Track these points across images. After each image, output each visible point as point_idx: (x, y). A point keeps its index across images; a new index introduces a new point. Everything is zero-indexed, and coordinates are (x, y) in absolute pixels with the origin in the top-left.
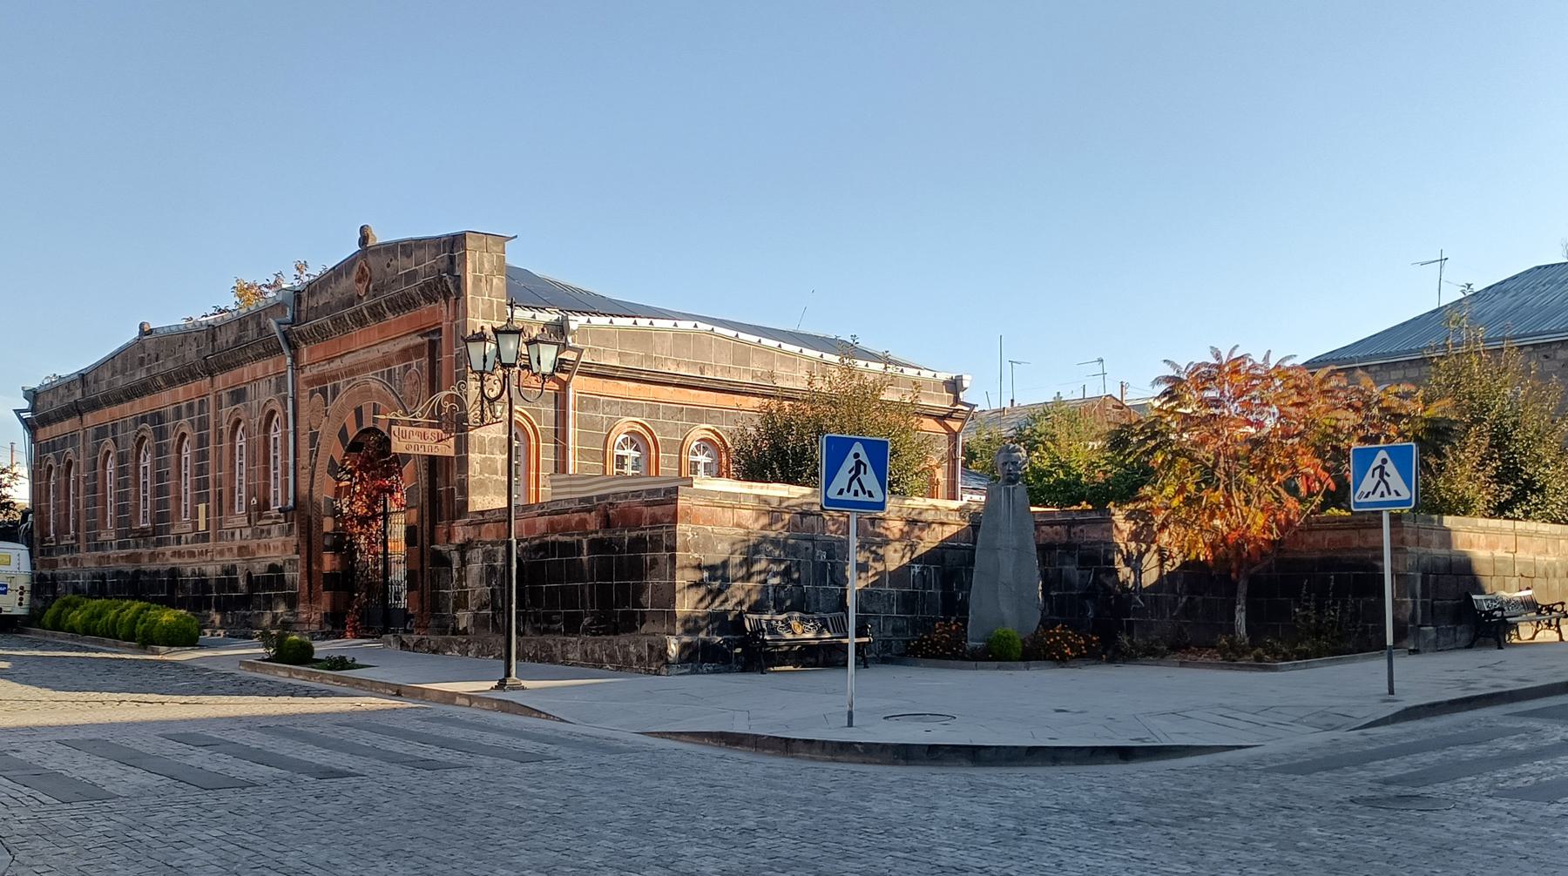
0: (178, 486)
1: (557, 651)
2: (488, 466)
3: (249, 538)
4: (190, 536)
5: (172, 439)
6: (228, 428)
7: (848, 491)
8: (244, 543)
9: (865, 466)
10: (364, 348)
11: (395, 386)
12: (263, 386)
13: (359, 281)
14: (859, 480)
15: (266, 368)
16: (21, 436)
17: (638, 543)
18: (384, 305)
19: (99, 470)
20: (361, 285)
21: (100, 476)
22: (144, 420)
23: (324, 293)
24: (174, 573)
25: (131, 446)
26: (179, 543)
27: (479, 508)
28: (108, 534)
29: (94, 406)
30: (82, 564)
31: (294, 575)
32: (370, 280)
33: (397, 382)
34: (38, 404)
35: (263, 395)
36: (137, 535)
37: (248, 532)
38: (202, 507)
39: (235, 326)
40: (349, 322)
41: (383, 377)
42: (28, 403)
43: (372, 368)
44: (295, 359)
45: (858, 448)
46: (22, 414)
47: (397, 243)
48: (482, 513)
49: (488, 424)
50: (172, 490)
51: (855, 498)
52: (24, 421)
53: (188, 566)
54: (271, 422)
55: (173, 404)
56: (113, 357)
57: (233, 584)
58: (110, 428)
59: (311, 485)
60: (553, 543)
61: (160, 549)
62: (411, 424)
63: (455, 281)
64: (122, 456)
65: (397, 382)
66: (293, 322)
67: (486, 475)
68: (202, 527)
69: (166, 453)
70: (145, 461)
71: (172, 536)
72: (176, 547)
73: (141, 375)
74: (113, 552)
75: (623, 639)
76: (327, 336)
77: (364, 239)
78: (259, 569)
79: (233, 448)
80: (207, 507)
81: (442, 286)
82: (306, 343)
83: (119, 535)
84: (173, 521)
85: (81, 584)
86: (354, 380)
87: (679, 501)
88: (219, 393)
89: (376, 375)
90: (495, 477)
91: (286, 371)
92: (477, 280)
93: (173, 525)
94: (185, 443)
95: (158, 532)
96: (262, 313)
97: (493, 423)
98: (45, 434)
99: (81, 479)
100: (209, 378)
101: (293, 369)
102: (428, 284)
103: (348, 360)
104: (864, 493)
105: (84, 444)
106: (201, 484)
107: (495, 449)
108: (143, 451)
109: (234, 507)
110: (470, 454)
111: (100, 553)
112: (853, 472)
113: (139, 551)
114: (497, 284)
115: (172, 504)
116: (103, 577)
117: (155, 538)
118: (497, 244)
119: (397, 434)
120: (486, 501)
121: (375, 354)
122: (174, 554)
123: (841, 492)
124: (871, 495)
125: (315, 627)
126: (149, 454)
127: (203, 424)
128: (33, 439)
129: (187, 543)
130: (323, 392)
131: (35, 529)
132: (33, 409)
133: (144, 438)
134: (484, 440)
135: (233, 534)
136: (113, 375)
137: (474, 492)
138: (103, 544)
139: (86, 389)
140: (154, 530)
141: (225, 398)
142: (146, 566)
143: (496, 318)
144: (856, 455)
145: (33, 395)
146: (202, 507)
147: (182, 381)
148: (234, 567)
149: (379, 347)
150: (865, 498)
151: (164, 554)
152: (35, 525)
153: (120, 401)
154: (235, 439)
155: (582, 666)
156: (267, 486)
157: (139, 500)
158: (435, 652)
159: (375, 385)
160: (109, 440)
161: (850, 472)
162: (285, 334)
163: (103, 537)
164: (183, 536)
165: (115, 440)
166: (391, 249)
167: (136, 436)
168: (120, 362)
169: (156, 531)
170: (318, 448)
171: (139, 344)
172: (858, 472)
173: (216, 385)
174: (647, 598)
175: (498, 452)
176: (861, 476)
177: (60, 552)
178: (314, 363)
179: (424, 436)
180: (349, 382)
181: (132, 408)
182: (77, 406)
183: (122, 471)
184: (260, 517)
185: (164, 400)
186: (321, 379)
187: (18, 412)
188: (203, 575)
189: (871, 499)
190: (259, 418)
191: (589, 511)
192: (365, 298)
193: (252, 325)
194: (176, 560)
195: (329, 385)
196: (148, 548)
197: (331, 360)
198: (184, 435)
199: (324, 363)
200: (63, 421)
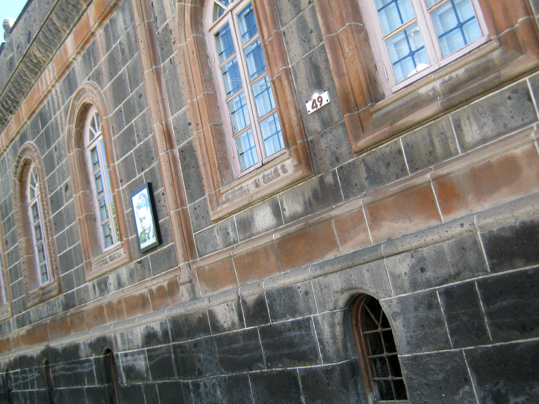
4: (124, 273)
6: (182, 10)
36: (37, 300)
55: (60, 78)
64: (5, 205)
69: (60, 158)
70: (33, 196)
71: (90, 284)
84: (87, 257)
93: (89, 265)
94: (88, 127)
108: (29, 185)
117: (61, 297)
126: (37, 185)
133: (27, 163)
140: (59, 285)
157: (33, 252)
164: (112, 279)
167: (17, 167)
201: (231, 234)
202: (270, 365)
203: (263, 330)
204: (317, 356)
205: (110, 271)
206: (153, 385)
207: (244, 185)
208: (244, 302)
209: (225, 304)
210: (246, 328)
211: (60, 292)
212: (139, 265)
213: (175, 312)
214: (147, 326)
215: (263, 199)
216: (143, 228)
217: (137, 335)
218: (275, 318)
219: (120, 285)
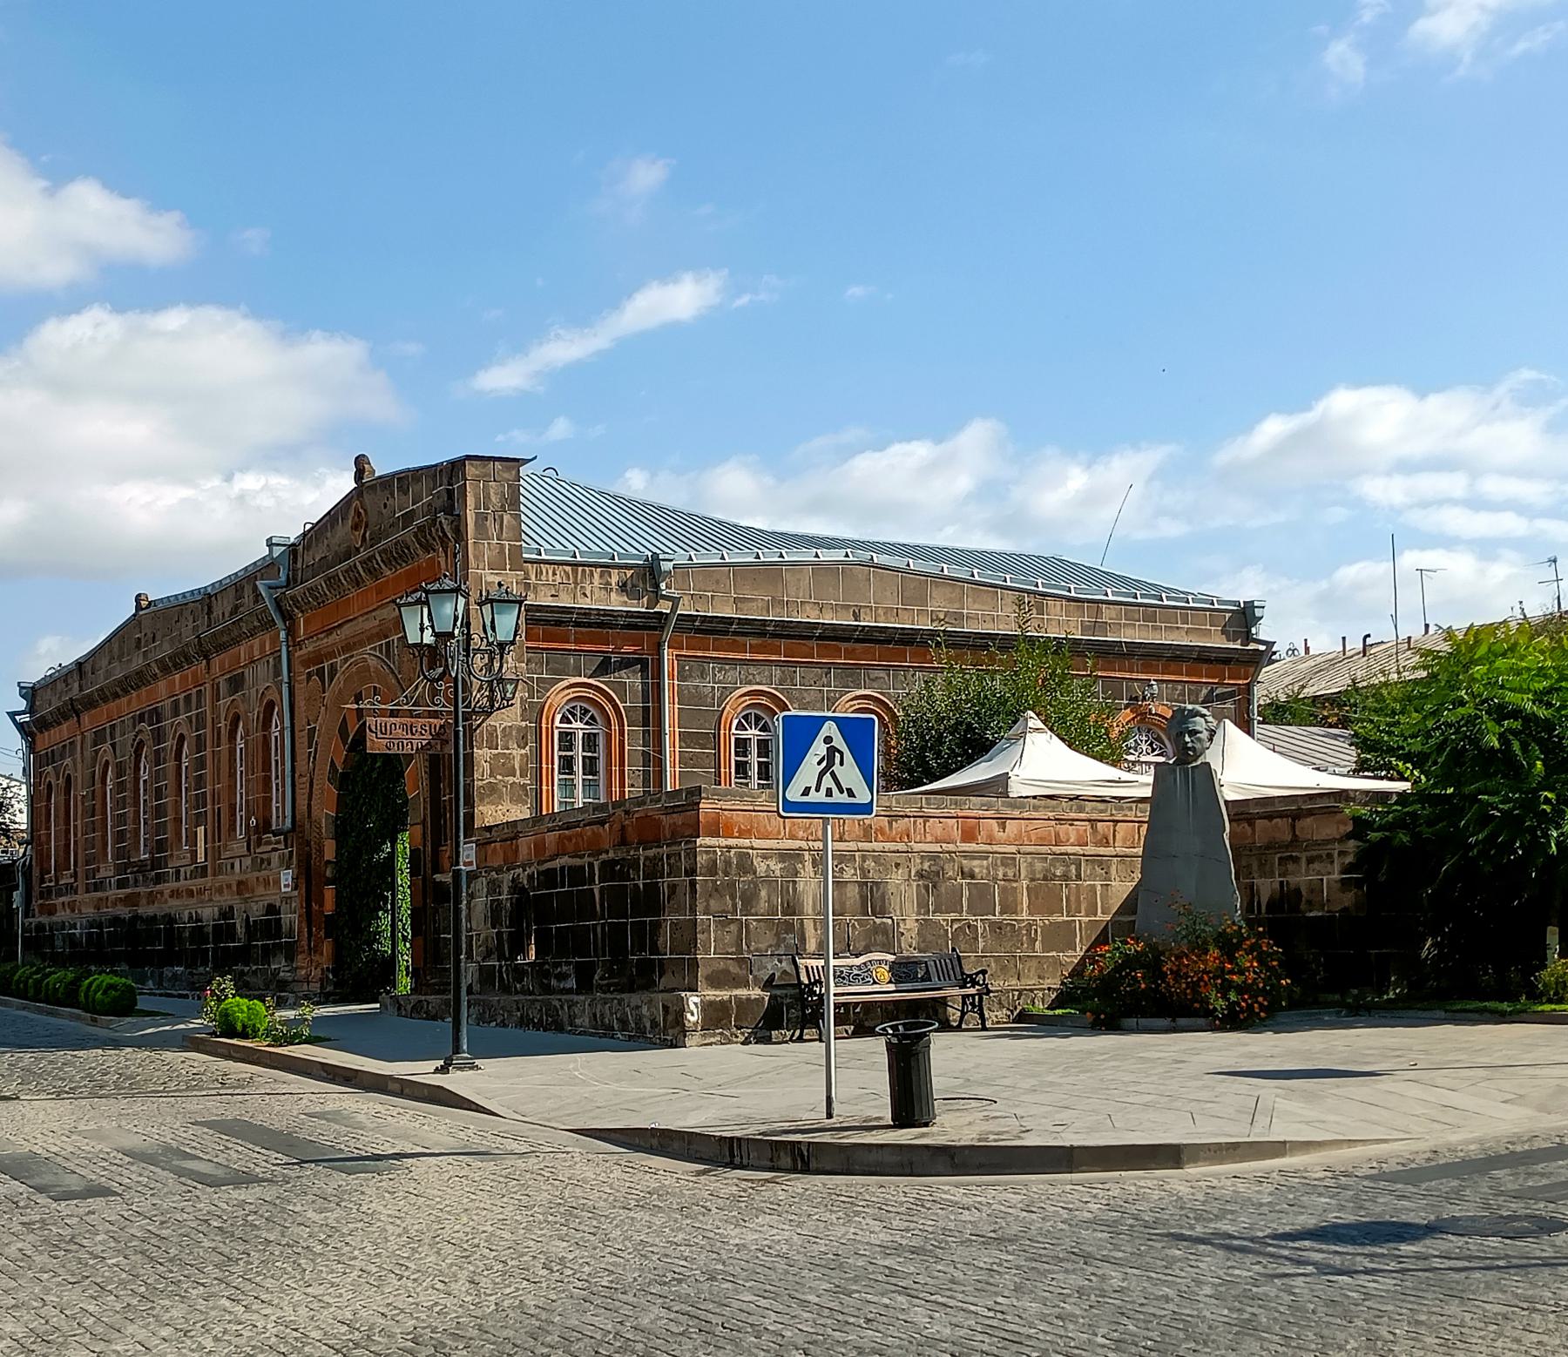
0: (177, 804)
1: (564, 1015)
2: (502, 766)
4: (189, 869)
5: (170, 743)
7: (817, 790)
8: (243, 877)
9: (841, 753)
10: (361, 615)
11: (394, 663)
12: (262, 669)
13: (356, 527)
14: (833, 775)
15: (262, 646)
16: (16, 741)
17: (654, 869)
18: (379, 559)
19: (98, 785)
20: (357, 533)
21: (98, 794)
22: (141, 718)
23: (320, 545)
24: (170, 919)
25: (127, 757)
26: (178, 879)
27: (489, 822)
28: (106, 871)
29: (90, 703)
30: (80, 910)
31: (290, 918)
32: (366, 526)
33: (396, 657)
34: (37, 703)
35: (259, 679)
36: (135, 869)
37: (248, 861)
38: (201, 830)
39: (232, 592)
40: (343, 581)
41: (381, 652)
42: (25, 702)
43: (370, 640)
44: (291, 632)
45: (830, 729)
46: (17, 718)
47: (393, 475)
48: (489, 829)
49: (499, 709)
50: (170, 810)
51: (829, 800)
52: (21, 727)
53: (183, 909)
54: (272, 714)
56: (108, 640)
57: (230, 932)
58: (108, 731)
59: (310, 799)
60: (562, 868)
61: (158, 887)
62: (393, 714)
63: (452, 522)
65: (396, 657)
66: (287, 585)
67: (499, 777)
68: (201, 858)
72: (173, 885)
73: (137, 662)
74: (114, 893)
75: (635, 999)
76: (323, 602)
77: (359, 475)
78: (257, 911)
79: (232, 752)
80: (206, 830)
81: (437, 530)
82: (302, 612)
83: (120, 869)
84: (172, 850)
85: (78, 935)
86: (352, 656)
87: (701, 806)
88: (217, 680)
89: (374, 649)
90: (511, 779)
91: (280, 650)
92: (481, 519)
95: (154, 870)
96: (258, 574)
97: (504, 707)
98: (47, 740)
99: (79, 798)
100: (204, 661)
101: (288, 646)
102: (421, 528)
103: (347, 631)
104: (842, 792)
105: (82, 753)
106: (200, 801)
107: (510, 743)
109: (235, 830)
110: (475, 750)
111: (99, 894)
112: (824, 764)
113: (137, 890)
114: (508, 522)
115: (170, 827)
116: (100, 926)
117: (153, 873)
118: (508, 469)
119: (373, 728)
120: (499, 812)
121: (371, 624)
122: (175, 894)
123: (806, 792)
124: (851, 793)
125: (316, 987)
127: (200, 722)
128: (32, 747)
129: (186, 879)
130: (320, 673)
131: (34, 863)
132: (31, 709)
134: (496, 731)
135: (232, 867)
136: (110, 663)
137: (482, 800)
138: (101, 882)
139: (84, 682)
141: (223, 688)
142: (145, 910)
143: (508, 567)
144: (828, 740)
145: (31, 693)
146: (201, 830)
147: (178, 666)
148: (231, 908)
149: (377, 612)
150: (843, 798)
151: (162, 893)
152: (34, 857)
153: (116, 696)
154: (236, 740)
155: (592, 1035)
156: (268, 800)
158: (434, 1018)
159: (372, 662)
160: (107, 746)
161: (819, 763)
162: (277, 602)
163: (102, 874)
164: (182, 869)
165: (113, 746)
166: (386, 482)
167: (134, 740)
168: (117, 645)
169: (156, 863)
170: (316, 749)
171: (134, 622)
172: (831, 764)
173: (212, 671)
174: (666, 938)
175: (515, 746)
176: (836, 768)
177: (60, 894)
178: (312, 637)
179: (410, 729)
180: (346, 660)
181: (129, 702)
182: (72, 704)
183: (120, 787)
184: (259, 843)
185: (162, 691)
186: (317, 658)
187: (12, 715)
189: (852, 800)
190: (256, 711)
191: (602, 823)
192: (362, 550)
193: (248, 591)
194: (174, 902)
195: (326, 664)
196: (147, 887)
197: (329, 632)
198: (182, 738)
199: (322, 636)
200: (59, 724)
211: (152, 870)
219: (186, 879)
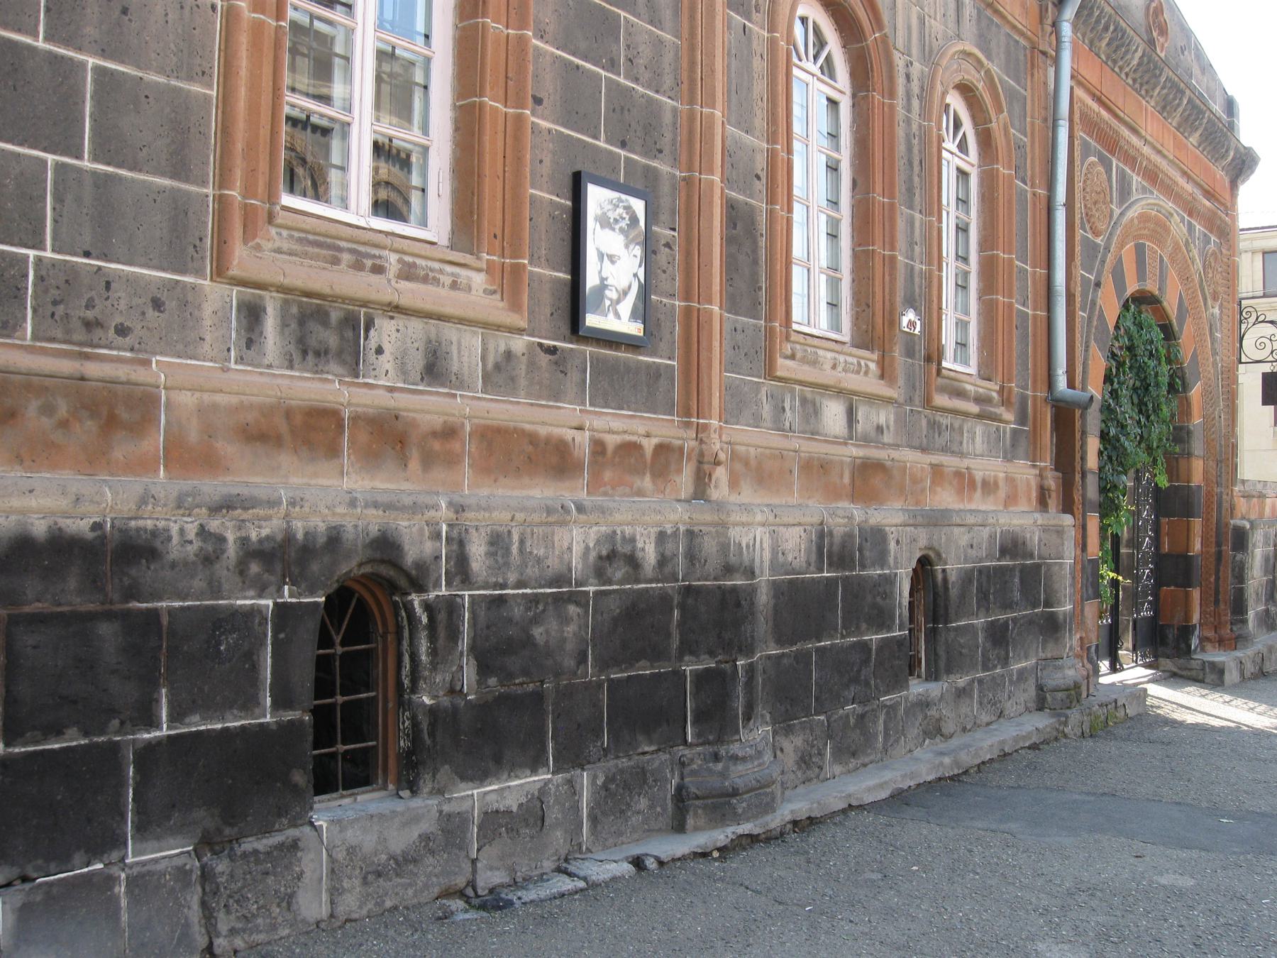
3: (887, 438)
188: (728, 570)
201: (788, 412)
202: (844, 633)
203: (846, 580)
204: (894, 621)
205: (395, 310)
206: (599, 685)
207: (821, 352)
208: (831, 533)
209: (802, 528)
210: (825, 574)
212: (544, 359)
213: (738, 518)
214: (614, 532)
215: (840, 392)
216: (603, 280)
217: (570, 549)
218: (863, 567)
